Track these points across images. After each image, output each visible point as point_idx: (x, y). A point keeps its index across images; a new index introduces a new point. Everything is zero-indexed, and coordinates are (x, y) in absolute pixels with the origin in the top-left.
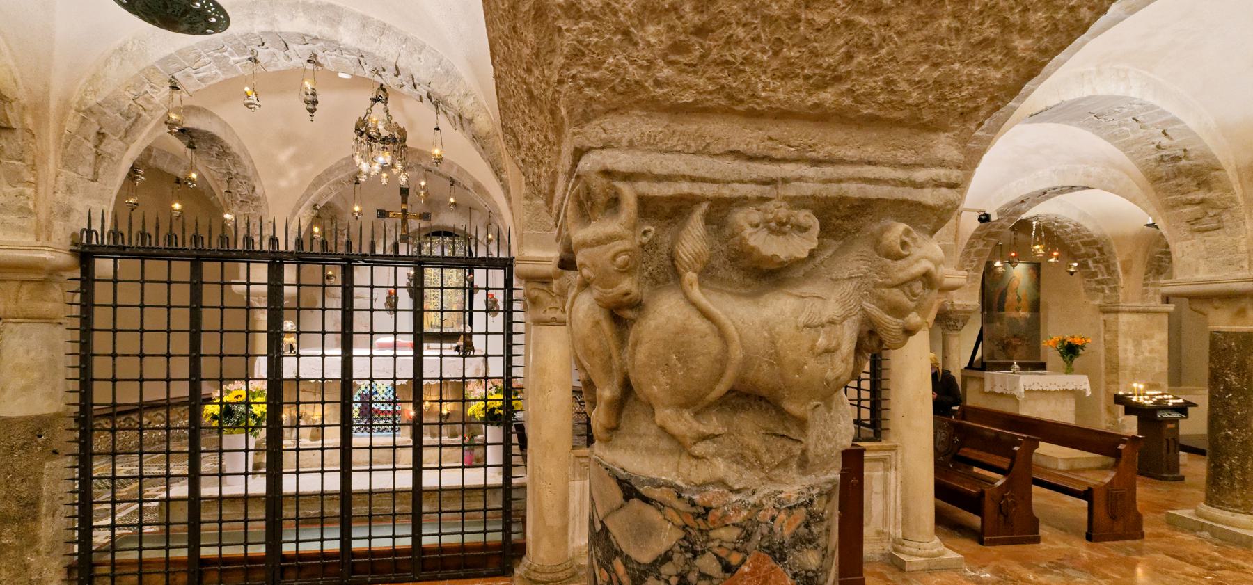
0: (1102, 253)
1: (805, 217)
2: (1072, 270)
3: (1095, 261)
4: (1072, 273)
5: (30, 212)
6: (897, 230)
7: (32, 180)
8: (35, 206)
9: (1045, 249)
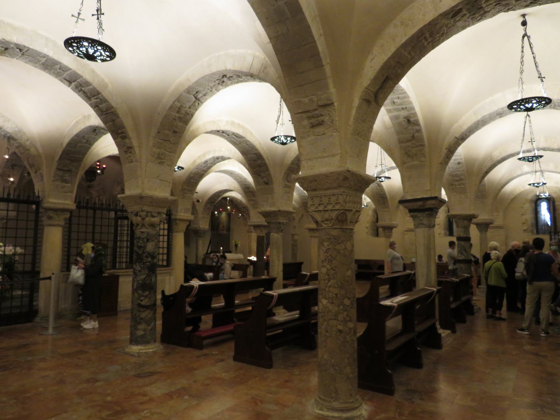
0: (248, 212)
1: (157, 213)
2: (239, 217)
3: (246, 214)
4: (239, 218)
6: (162, 214)
9: (231, 208)
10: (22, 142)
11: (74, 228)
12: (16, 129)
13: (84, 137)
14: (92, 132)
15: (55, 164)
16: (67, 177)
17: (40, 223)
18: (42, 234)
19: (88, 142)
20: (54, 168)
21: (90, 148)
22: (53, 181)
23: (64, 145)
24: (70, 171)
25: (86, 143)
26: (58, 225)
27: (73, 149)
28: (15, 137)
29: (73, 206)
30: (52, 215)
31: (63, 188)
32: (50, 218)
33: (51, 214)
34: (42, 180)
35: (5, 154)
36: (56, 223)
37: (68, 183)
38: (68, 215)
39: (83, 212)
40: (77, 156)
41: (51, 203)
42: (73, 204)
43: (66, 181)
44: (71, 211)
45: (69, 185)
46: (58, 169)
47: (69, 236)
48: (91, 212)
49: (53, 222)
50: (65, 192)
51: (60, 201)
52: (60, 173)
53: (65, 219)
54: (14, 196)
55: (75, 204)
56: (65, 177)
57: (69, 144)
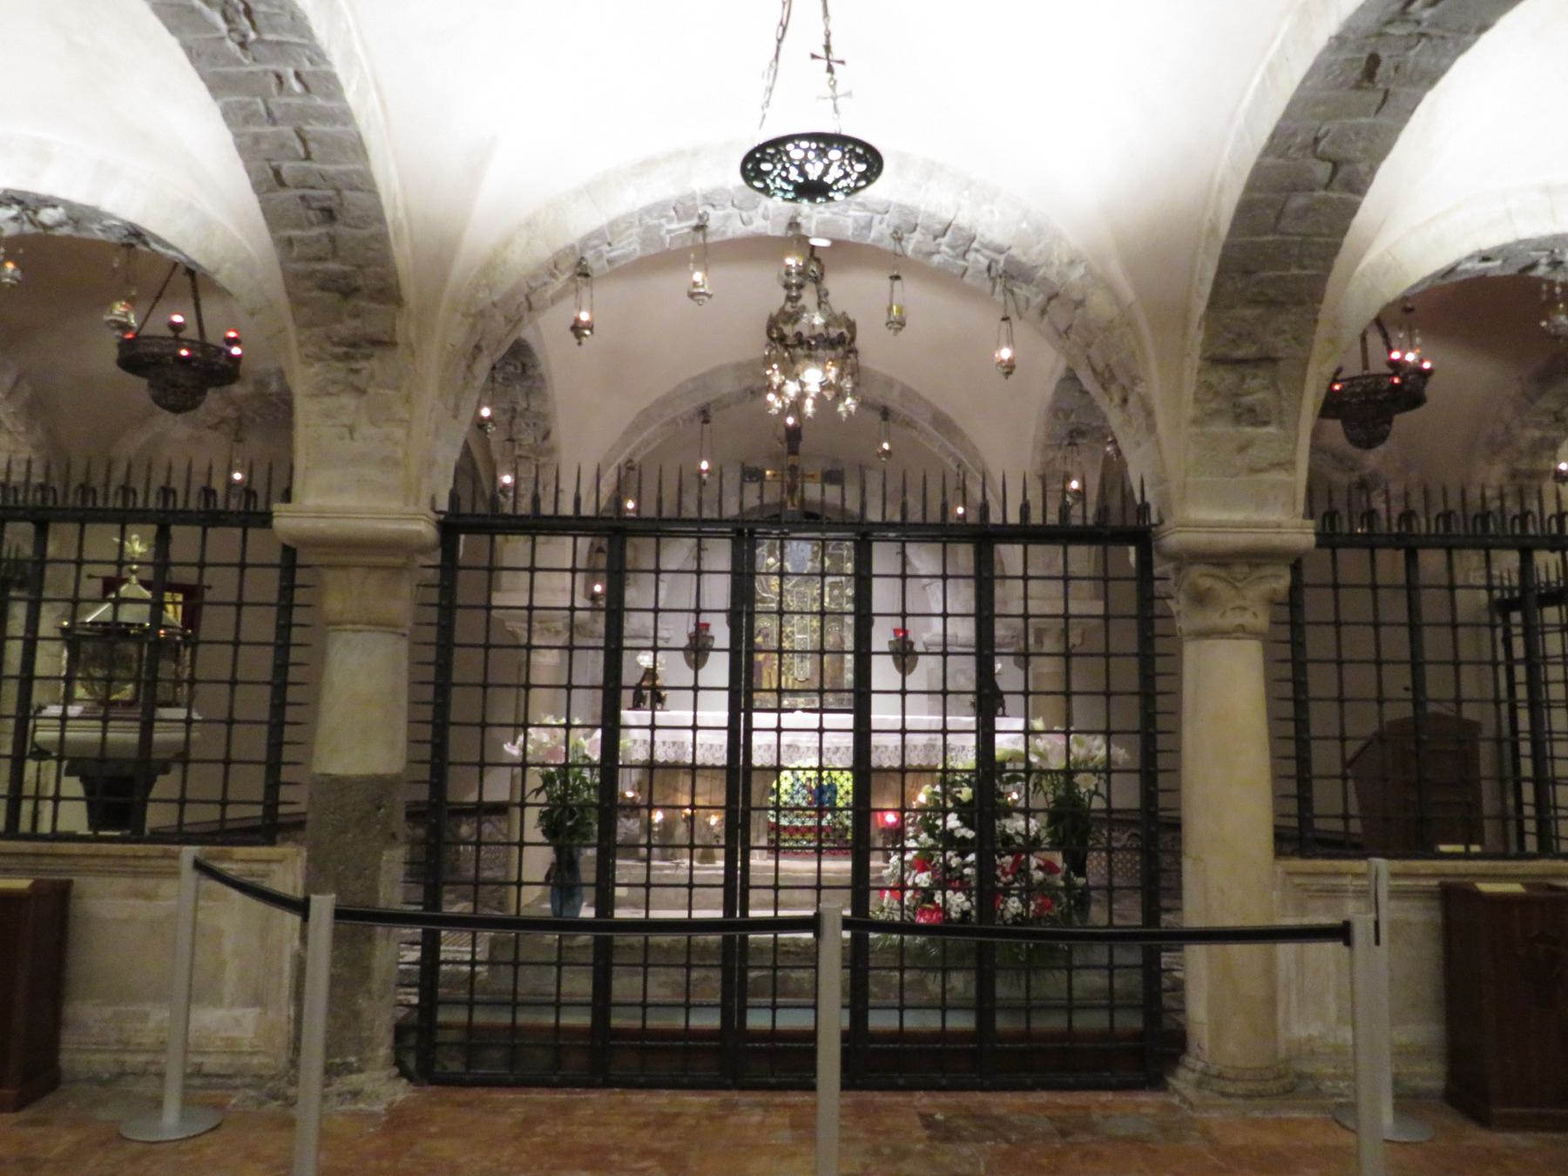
5: (396, 464)
7: (407, 416)
8: (406, 454)
10: (1052, 274)
11: (1319, 643)
12: (1024, 225)
13: (1317, 140)
14: (1358, 86)
15: (1197, 336)
16: (1257, 391)
17: (1159, 626)
18: (1176, 674)
19: (1340, 175)
20: (1194, 360)
21: (1352, 210)
22: (1195, 422)
23: (1224, 227)
24: (1267, 360)
25: (1327, 186)
26: (1241, 632)
27: (1270, 238)
28: (1024, 259)
29: (1300, 534)
30: (1206, 583)
31: (1242, 449)
32: (1201, 599)
33: (1200, 577)
34: (1151, 428)
35: (998, 346)
36: (1233, 620)
37: (1266, 423)
38: (1283, 582)
39: (1352, 563)
40: (1295, 271)
41: (1198, 525)
42: (1299, 521)
43: (1253, 416)
44: (1296, 563)
45: (1271, 429)
46: (1215, 361)
47: (1299, 685)
48: (1391, 563)
49: (1213, 619)
50: (1254, 470)
51: (1238, 516)
52: (1225, 378)
53: (1272, 602)
55: (1310, 523)
56: (1248, 393)
57: (1246, 209)
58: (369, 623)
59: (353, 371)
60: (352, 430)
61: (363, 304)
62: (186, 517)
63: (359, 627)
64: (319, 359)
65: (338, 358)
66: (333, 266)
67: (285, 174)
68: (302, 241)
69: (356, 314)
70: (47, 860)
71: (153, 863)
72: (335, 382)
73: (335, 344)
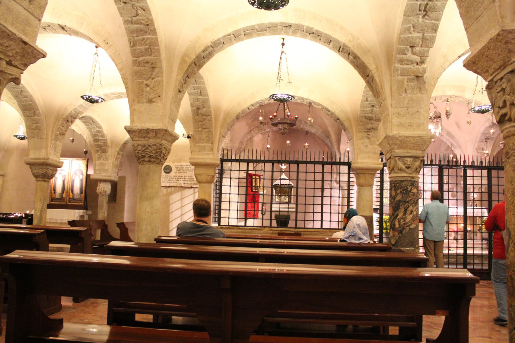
54: (494, 165)
58: (369, 185)
59: (368, 134)
60: (367, 146)
61: (373, 122)
62: (327, 163)
63: (367, 186)
64: (361, 132)
65: (365, 132)
66: (370, 115)
67: (368, 100)
68: (366, 111)
69: (371, 124)
70: (306, 232)
71: (327, 233)
72: (364, 137)
73: (365, 129)
